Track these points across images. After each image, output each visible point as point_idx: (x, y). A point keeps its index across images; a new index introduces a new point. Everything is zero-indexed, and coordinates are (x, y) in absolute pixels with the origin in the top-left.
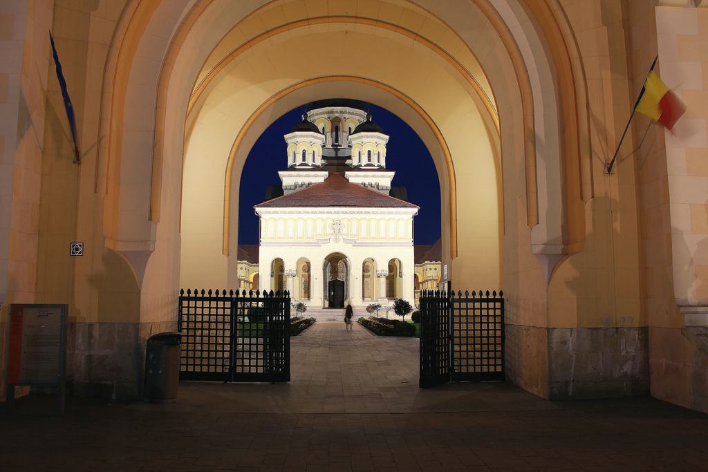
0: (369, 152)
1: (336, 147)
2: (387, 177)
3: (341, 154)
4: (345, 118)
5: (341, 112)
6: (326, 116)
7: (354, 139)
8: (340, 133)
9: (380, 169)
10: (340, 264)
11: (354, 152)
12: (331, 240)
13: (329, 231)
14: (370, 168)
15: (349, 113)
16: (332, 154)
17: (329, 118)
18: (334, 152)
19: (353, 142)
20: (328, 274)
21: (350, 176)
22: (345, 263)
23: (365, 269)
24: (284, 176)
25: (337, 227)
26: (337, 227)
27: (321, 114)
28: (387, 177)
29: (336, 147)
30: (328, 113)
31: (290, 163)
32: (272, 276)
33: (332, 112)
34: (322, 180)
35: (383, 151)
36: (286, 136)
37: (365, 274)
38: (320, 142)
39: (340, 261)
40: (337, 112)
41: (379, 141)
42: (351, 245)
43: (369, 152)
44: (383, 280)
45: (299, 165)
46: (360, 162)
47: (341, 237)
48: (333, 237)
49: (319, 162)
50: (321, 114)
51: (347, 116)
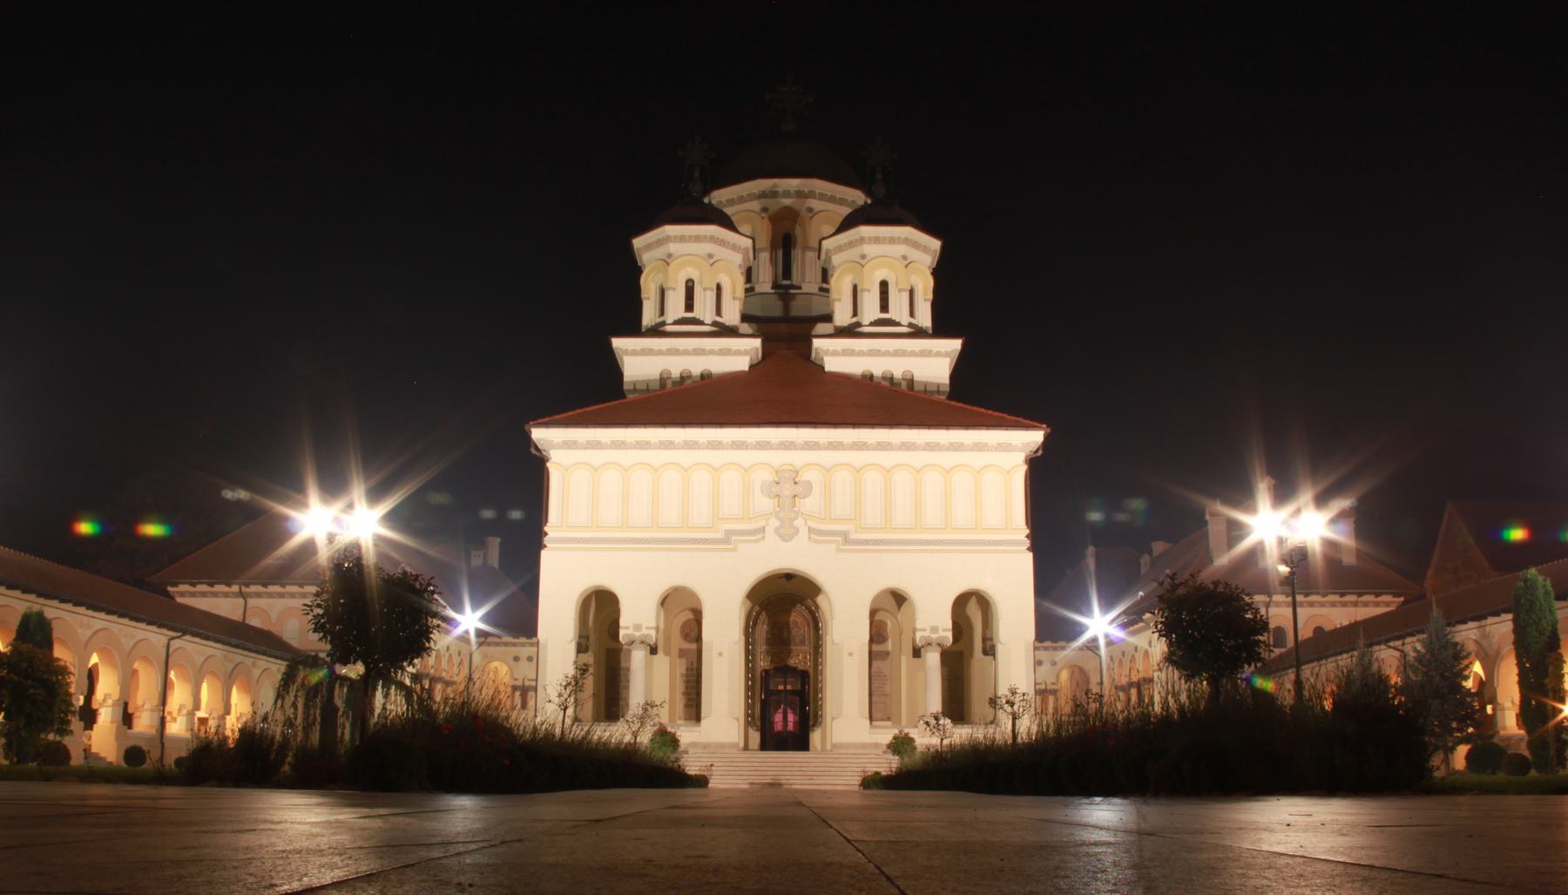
0: (884, 285)
1: (784, 289)
2: (939, 354)
3: (797, 309)
4: (810, 210)
5: (800, 195)
6: (756, 205)
7: (840, 249)
8: (797, 253)
9: (918, 333)
10: (797, 617)
11: (841, 286)
12: (769, 531)
13: (765, 504)
14: (885, 327)
15: (822, 197)
16: (776, 310)
17: (765, 210)
18: (779, 304)
19: (836, 259)
20: (761, 647)
21: (827, 353)
22: (809, 609)
23: (877, 634)
24: (627, 352)
25: (788, 489)
26: (788, 489)
27: (741, 200)
28: (939, 354)
29: (784, 289)
30: (763, 195)
31: (649, 317)
32: (581, 649)
33: (774, 194)
34: (741, 364)
35: (925, 285)
36: (638, 242)
37: (875, 648)
38: (737, 258)
39: (799, 608)
40: (787, 194)
41: (914, 254)
42: (834, 546)
43: (884, 285)
44: (933, 659)
45: (676, 323)
46: (855, 314)
47: (799, 523)
48: (774, 523)
49: (731, 316)
50: (741, 200)
51: (815, 204)
